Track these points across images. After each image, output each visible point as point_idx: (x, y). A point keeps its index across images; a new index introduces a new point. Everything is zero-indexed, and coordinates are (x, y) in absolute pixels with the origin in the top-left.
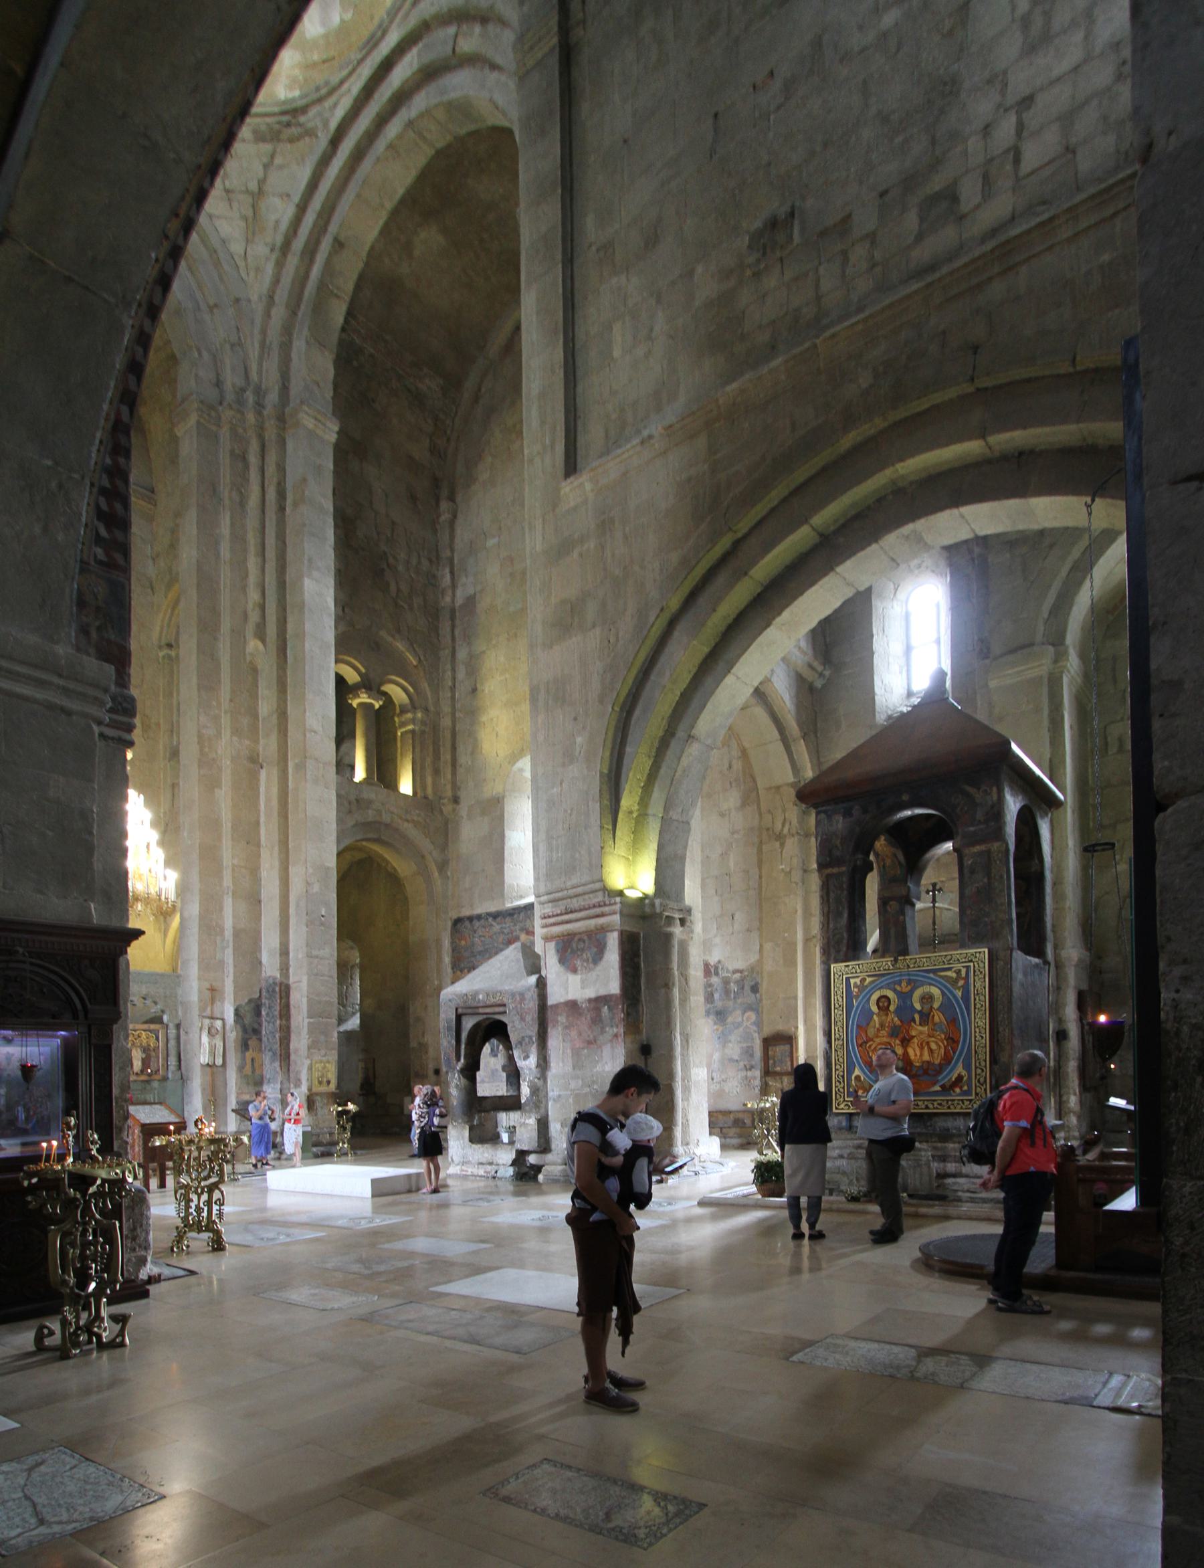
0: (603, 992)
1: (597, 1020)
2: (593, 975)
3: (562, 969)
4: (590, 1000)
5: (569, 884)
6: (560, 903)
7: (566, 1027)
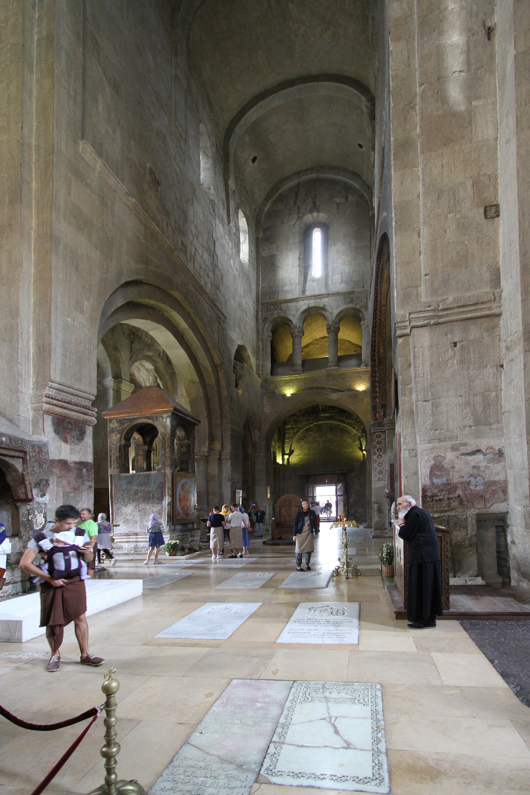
0: (83, 460)
1: (80, 476)
2: (78, 448)
3: (57, 437)
4: (76, 463)
5: (77, 387)
6: (63, 393)
7: (59, 477)
